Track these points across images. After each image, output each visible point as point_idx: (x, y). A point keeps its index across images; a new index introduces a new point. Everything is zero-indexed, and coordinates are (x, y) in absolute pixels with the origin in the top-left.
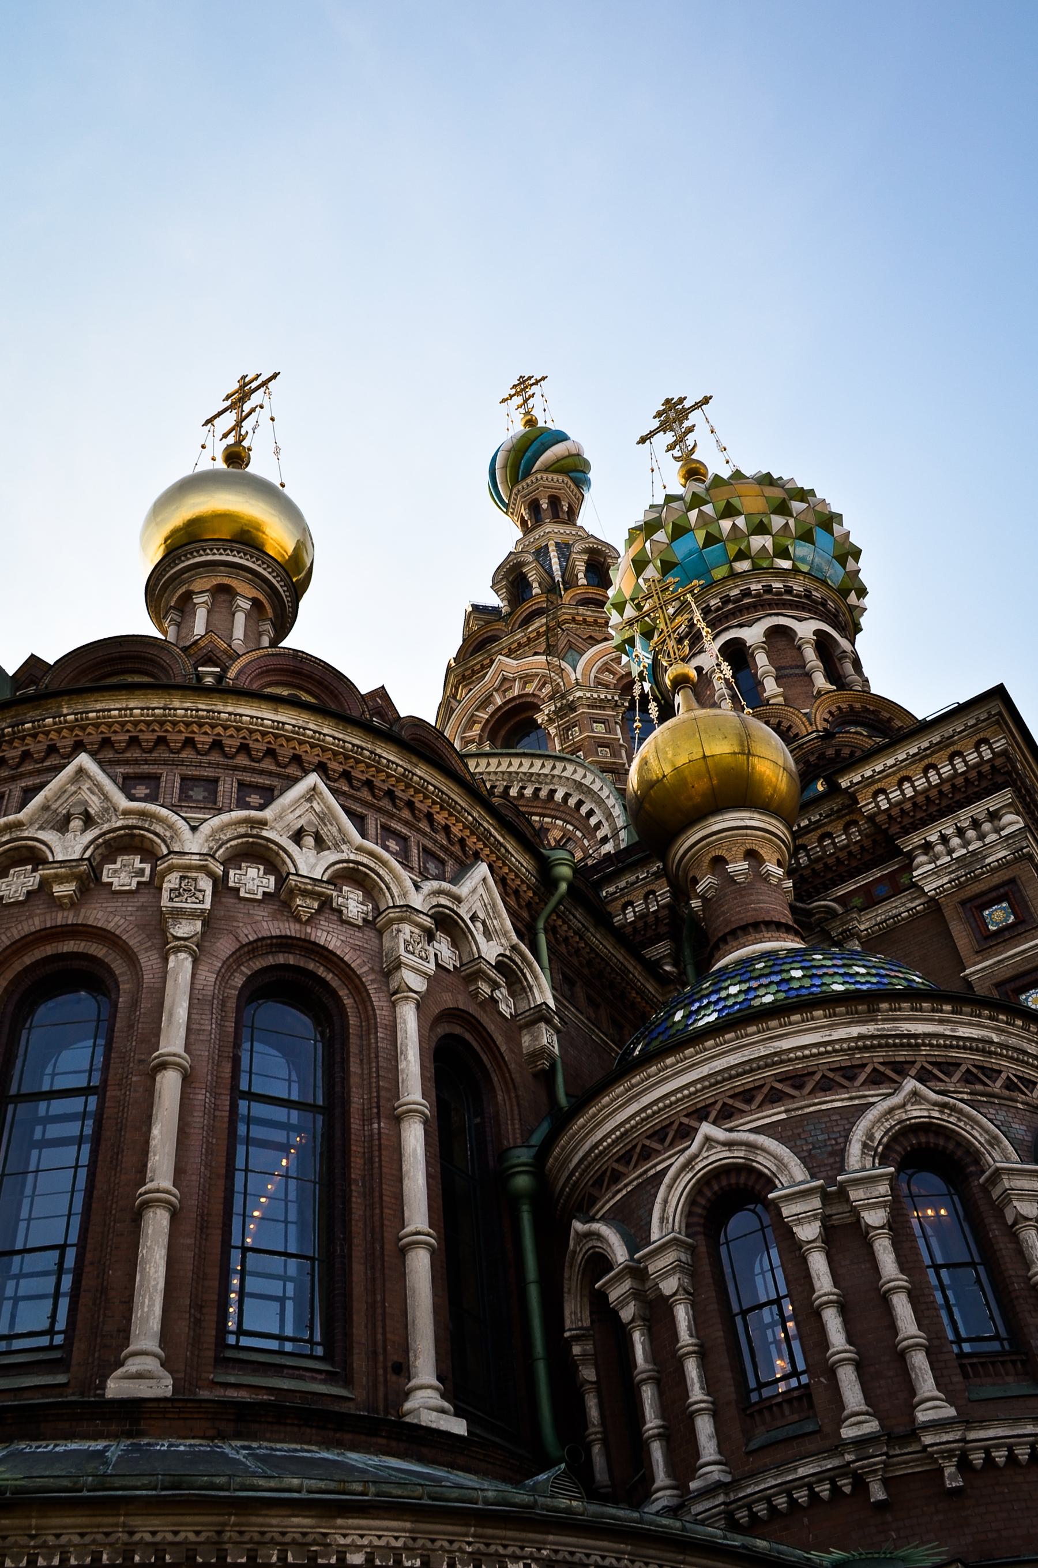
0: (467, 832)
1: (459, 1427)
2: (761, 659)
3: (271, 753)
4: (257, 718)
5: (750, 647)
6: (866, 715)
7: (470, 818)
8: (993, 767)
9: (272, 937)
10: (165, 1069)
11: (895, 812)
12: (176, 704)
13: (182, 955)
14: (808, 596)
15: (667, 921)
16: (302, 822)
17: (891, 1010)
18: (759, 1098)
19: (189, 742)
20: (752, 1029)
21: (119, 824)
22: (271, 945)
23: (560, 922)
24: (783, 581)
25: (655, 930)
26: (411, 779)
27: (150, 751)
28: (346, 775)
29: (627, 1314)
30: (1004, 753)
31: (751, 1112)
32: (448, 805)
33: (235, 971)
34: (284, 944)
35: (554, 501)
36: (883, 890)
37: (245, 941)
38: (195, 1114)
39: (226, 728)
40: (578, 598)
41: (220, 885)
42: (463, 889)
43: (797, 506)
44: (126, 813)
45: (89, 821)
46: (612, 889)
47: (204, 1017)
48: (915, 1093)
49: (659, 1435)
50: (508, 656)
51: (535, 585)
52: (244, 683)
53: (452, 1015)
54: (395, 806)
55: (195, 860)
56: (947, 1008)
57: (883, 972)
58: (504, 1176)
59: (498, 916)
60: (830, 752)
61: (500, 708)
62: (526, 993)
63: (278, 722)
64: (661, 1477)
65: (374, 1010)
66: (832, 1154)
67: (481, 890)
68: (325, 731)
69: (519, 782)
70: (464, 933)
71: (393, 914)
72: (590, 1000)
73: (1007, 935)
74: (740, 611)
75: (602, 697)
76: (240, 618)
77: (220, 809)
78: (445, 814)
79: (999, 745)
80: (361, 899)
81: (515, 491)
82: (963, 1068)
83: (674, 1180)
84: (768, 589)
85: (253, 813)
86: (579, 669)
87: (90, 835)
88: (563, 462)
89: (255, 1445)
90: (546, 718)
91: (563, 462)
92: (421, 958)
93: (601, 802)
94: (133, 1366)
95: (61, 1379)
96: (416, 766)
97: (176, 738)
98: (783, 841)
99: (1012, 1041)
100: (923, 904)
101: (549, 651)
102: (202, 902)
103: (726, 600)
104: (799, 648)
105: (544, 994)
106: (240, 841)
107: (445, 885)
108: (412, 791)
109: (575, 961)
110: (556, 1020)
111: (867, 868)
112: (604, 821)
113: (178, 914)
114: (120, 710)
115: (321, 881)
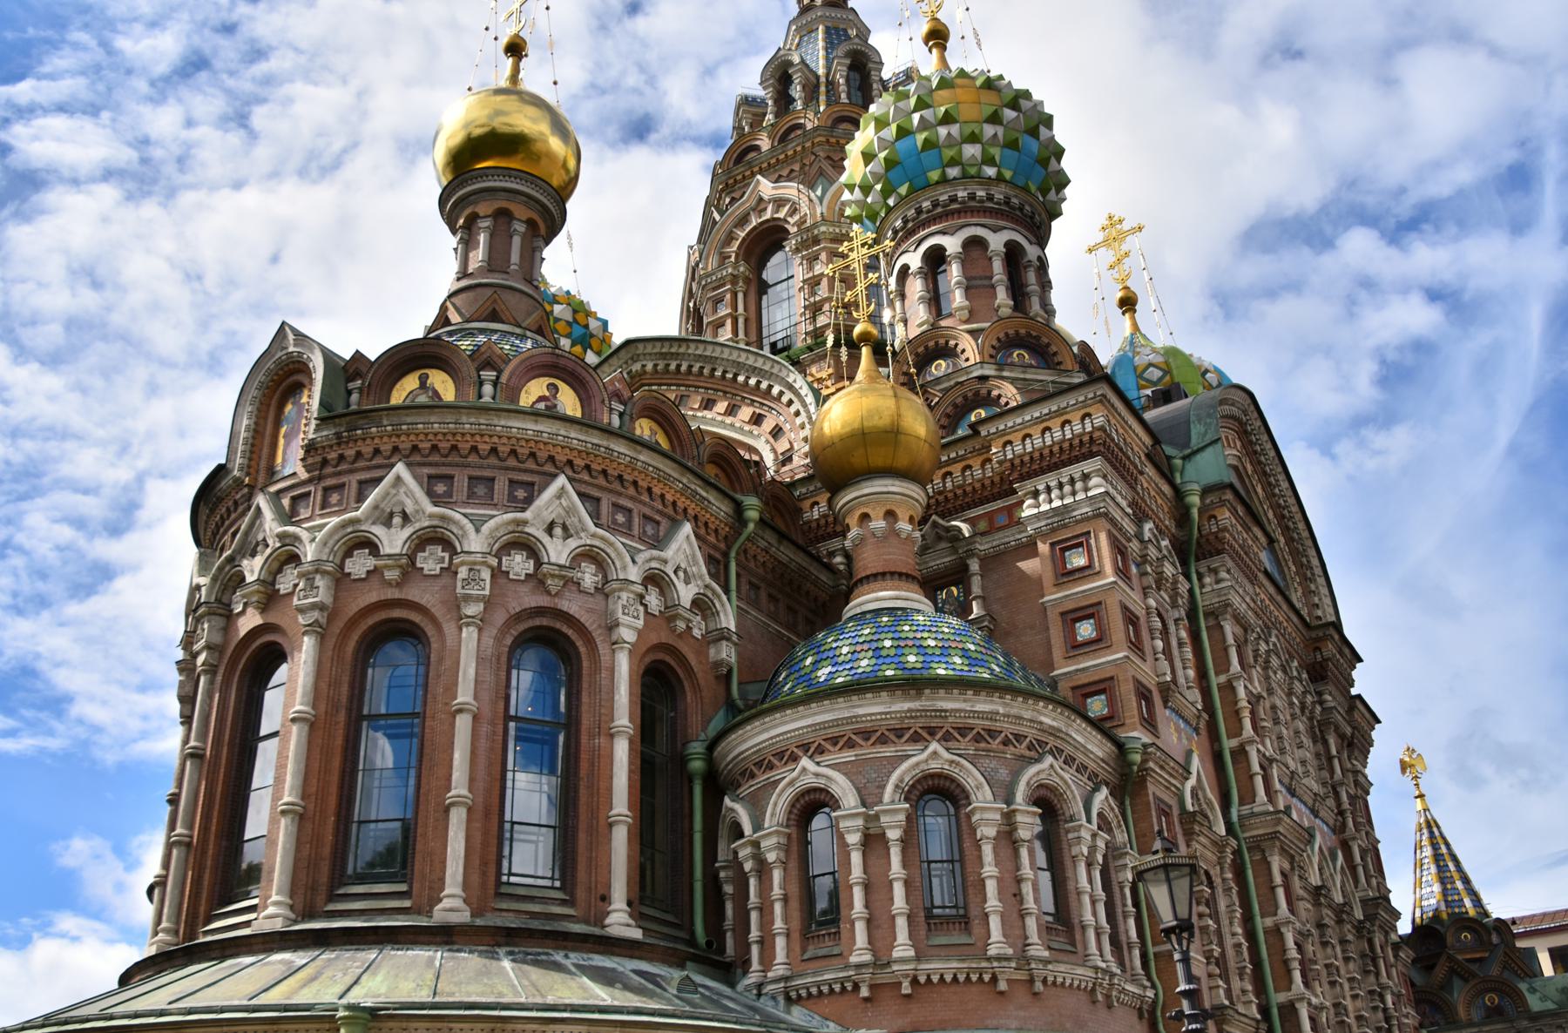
0: (678, 495)
1: (636, 934)
2: (954, 271)
3: (533, 455)
8: (1091, 438)
11: (1017, 462)
12: (464, 419)
13: (471, 629)
14: (1007, 202)
16: (553, 516)
18: (841, 744)
19: (474, 449)
20: (841, 700)
27: (446, 456)
29: (748, 866)
30: (1102, 429)
31: (834, 753)
32: (664, 478)
34: (540, 611)
36: (1002, 520)
37: (513, 612)
39: (500, 437)
40: (835, 116)
42: (669, 553)
43: (1009, 114)
44: (431, 516)
45: (406, 518)
46: (804, 490)
48: (935, 753)
49: (757, 942)
54: (623, 486)
55: (479, 558)
58: (683, 760)
59: (696, 563)
60: (984, 392)
64: (755, 965)
66: (878, 787)
67: (685, 546)
68: (572, 435)
71: (615, 585)
73: (1077, 575)
76: (517, 241)
78: (661, 485)
82: (975, 732)
83: (783, 791)
84: (972, 197)
85: (519, 515)
86: (825, 202)
87: (408, 531)
89: (516, 950)
93: (805, 405)
94: (446, 903)
95: (407, 903)
96: (640, 452)
97: (465, 447)
99: (1014, 711)
102: (483, 589)
103: (935, 204)
104: (990, 259)
107: (655, 553)
108: (636, 473)
110: (735, 638)
111: (994, 498)
113: (468, 598)
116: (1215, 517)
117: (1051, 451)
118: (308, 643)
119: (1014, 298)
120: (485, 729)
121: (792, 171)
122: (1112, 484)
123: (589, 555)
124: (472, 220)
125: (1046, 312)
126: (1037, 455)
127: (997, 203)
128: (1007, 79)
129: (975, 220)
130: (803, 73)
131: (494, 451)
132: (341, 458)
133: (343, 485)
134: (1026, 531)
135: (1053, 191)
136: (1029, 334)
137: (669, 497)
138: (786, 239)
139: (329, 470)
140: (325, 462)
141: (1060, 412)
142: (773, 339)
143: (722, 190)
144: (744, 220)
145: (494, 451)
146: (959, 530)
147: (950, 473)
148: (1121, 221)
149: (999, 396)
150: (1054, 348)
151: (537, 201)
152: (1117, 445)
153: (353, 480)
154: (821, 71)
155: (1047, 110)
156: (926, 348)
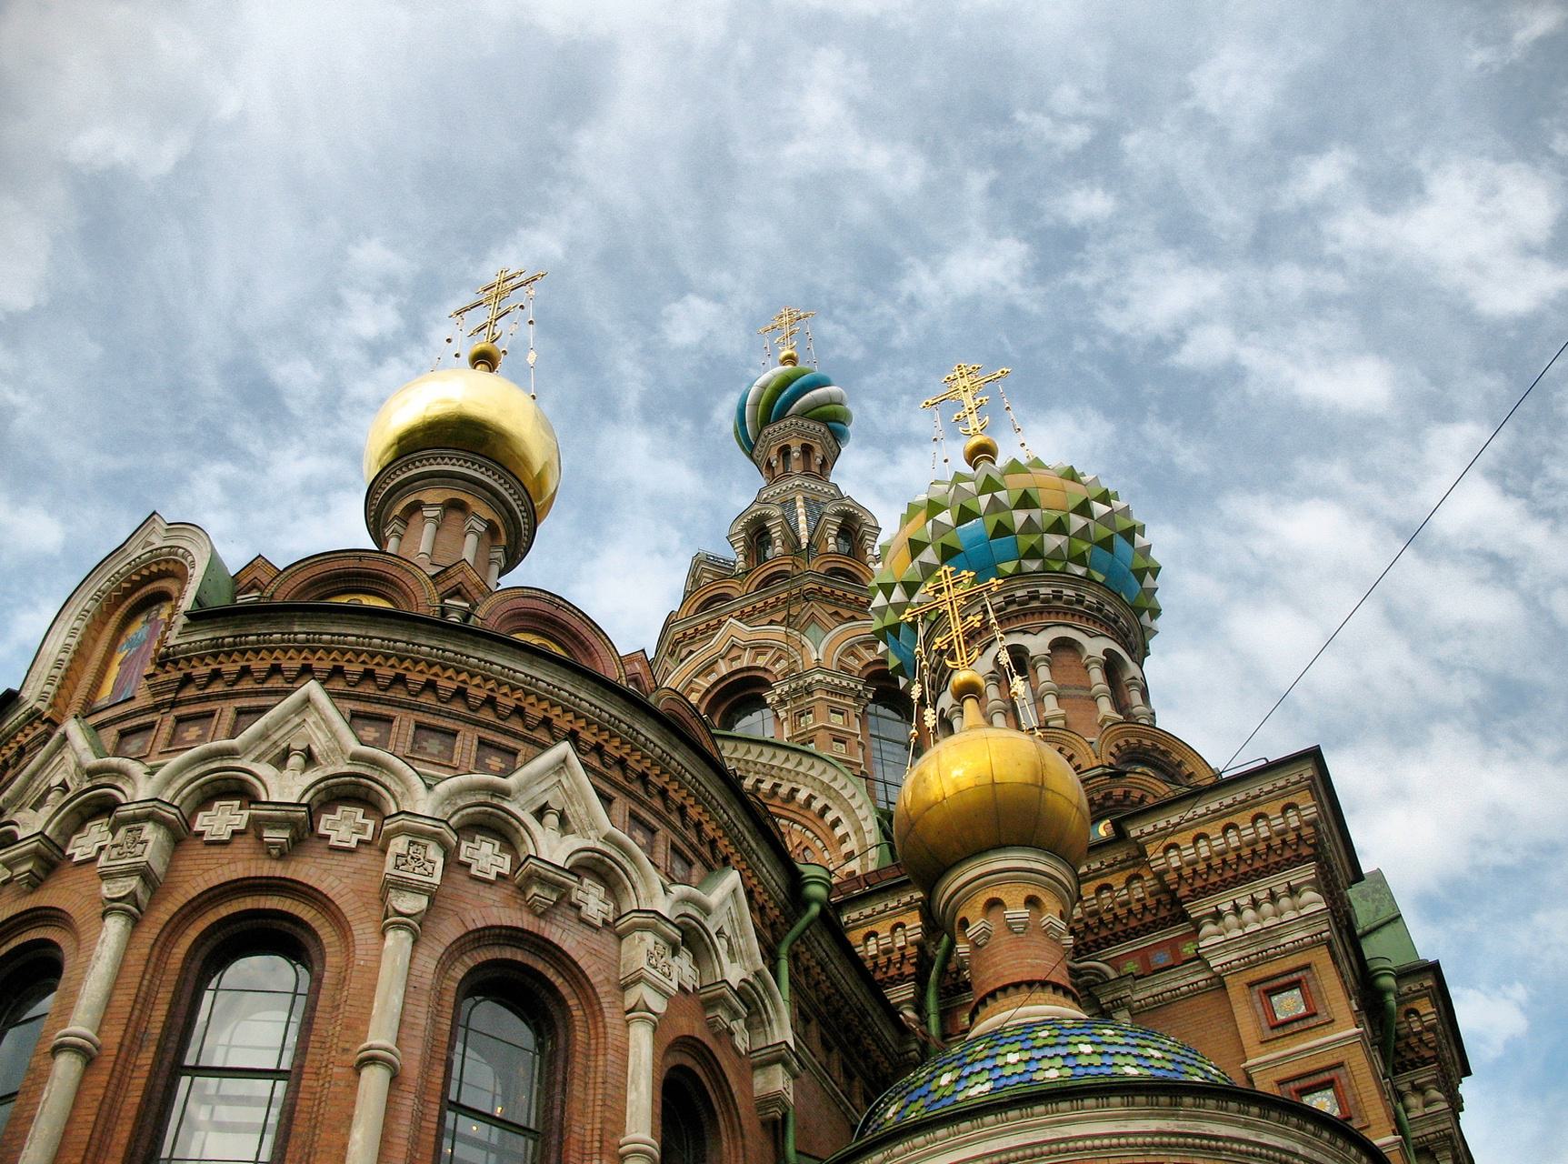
0: (720, 833)
2: (1043, 673)
4: (510, 669)
5: (1032, 658)
6: (1155, 754)
7: (725, 816)
9: (501, 927)
10: (374, 1064)
11: (1187, 871)
13: (403, 934)
15: (915, 960)
16: (547, 797)
17: (1194, 1106)
20: (1040, 1109)
21: (346, 769)
22: (499, 935)
23: (803, 949)
24: (1074, 589)
25: (899, 969)
26: (668, 764)
27: (386, 689)
28: (598, 749)
33: (456, 960)
34: (513, 936)
35: (807, 450)
37: (471, 927)
38: (401, 1121)
41: (453, 862)
43: (1099, 509)
44: (356, 758)
46: (855, 915)
47: (419, 1009)
50: (740, 620)
51: (778, 542)
52: (492, 625)
53: (687, 1044)
54: (647, 792)
55: (427, 825)
56: (1255, 1110)
57: (1179, 1059)
59: (744, 935)
60: (1118, 792)
62: (764, 1027)
63: (532, 677)
65: (605, 1027)
67: (730, 903)
69: (756, 773)
70: (708, 950)
72: (824, 1043)
73: (1296, 1026)
74: (1025, 615)
75: (845, 683)
77: (456, 769)
80: (602, 895)
84: (1058, 596)
86: (821, 649)
87: (312, 776)
90: (777, 698)
92: (664, 974)
93: (850, 812)
97: (416, 677)
98: (1068, 891)
100: (1206, 980)
101: (788, 622)
102: (430, 875)
104: (1087, 667)
105: (782, 1031)
106: (477, 809)
108: (666, 778)
109: (812, 994)
110: (795, 1063)
111: (1147, 929)
112: (851, 834)
113: (402, 886)
114: (358, 636)
115: (562, 869)
116: (1416, 1012)
118: (114, 928)
120: (408, 1103)
123: (595, 867)
124: (416, 507)
126: (1216, 861)
131: (461, 693)
132: (216, 675)
133: (211, 714)
134: (1209, 968)
137: (708, 828)
139: (191, 692)
140: (187, 680)
141: (1254, 801)
144: (708, 668)
145: (461, 693)
146: (1100, 973)
149: (1142, 799)
151: (504, 502)
153: (228, 709)
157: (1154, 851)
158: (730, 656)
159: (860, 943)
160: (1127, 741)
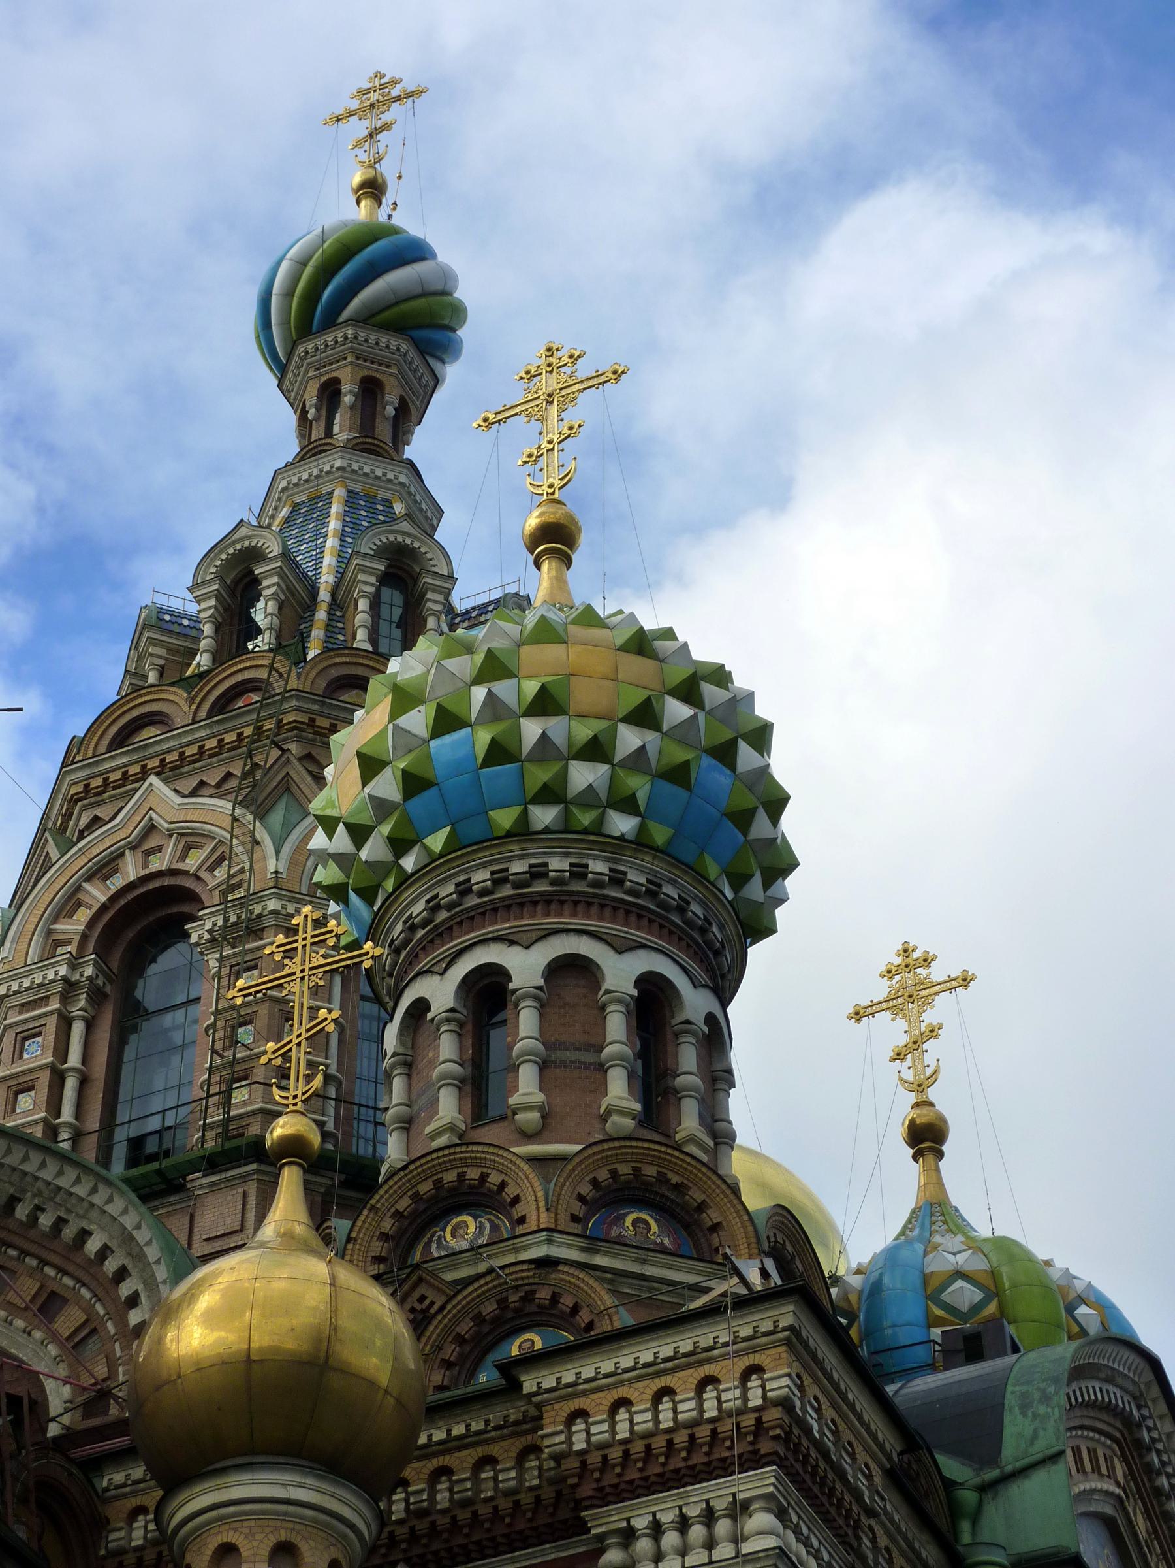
2: (527, 1021)
6: (663, 1190)
8: (759, 1421)
11: (594, 1459)
30: (785, 1404)
35: (370, 389)
40: (334, 673)
43: (677, 711)
46: (118, 1478)
60: (544, 1294)
61: (130, 887)
79: (779, 1386)
81: (301, 349)
84: (578, 872)
86: (287, 849)
88: (405, 307)
91: (405, 307)
103: (499, 880)
104: (603, 1008)
117: (670, 1443)
119: (647, 1102)
121: (229, 775)
122: (797, 1531)
125: (714, 1135)
127: (630, 892)
128: (682, 638)
129: (579, 922)
130: (282, 576)
135: (757, 880)
136: (662, 1179)
138: (195, 918)
142: (134, 1131)
143: (74, 800)
144: (105, 868)
147: (446, 1471)
148: (927, 961)
149: (575, 1309)
150: (713, 1215)
152: (819, 1445)
154: (326, 580)
155: (763, 710)
156: (438, 1184)
157: (552, 1425)
158: (146, 847)
159: (121, 1524)
160: (614, 1174)
